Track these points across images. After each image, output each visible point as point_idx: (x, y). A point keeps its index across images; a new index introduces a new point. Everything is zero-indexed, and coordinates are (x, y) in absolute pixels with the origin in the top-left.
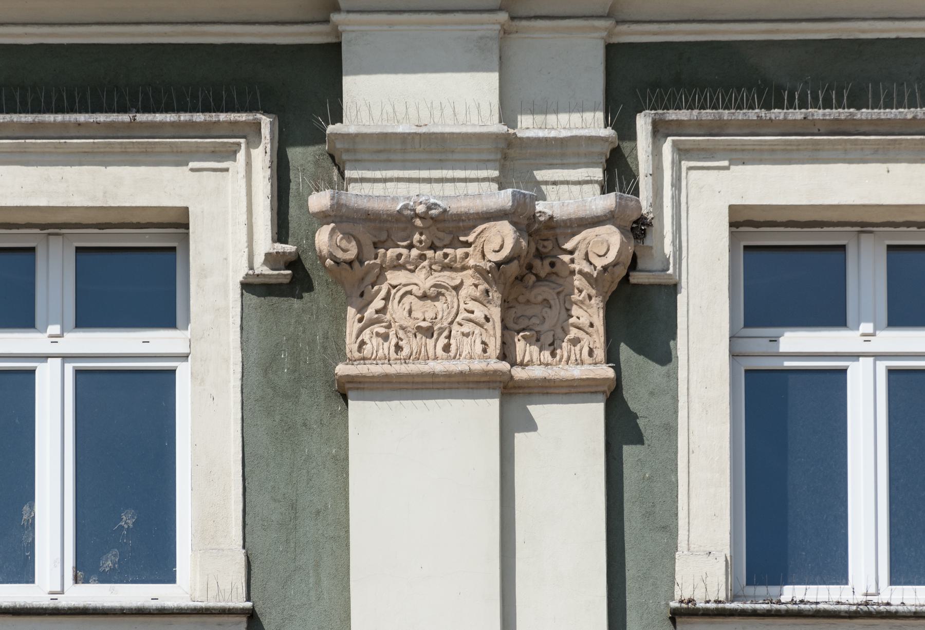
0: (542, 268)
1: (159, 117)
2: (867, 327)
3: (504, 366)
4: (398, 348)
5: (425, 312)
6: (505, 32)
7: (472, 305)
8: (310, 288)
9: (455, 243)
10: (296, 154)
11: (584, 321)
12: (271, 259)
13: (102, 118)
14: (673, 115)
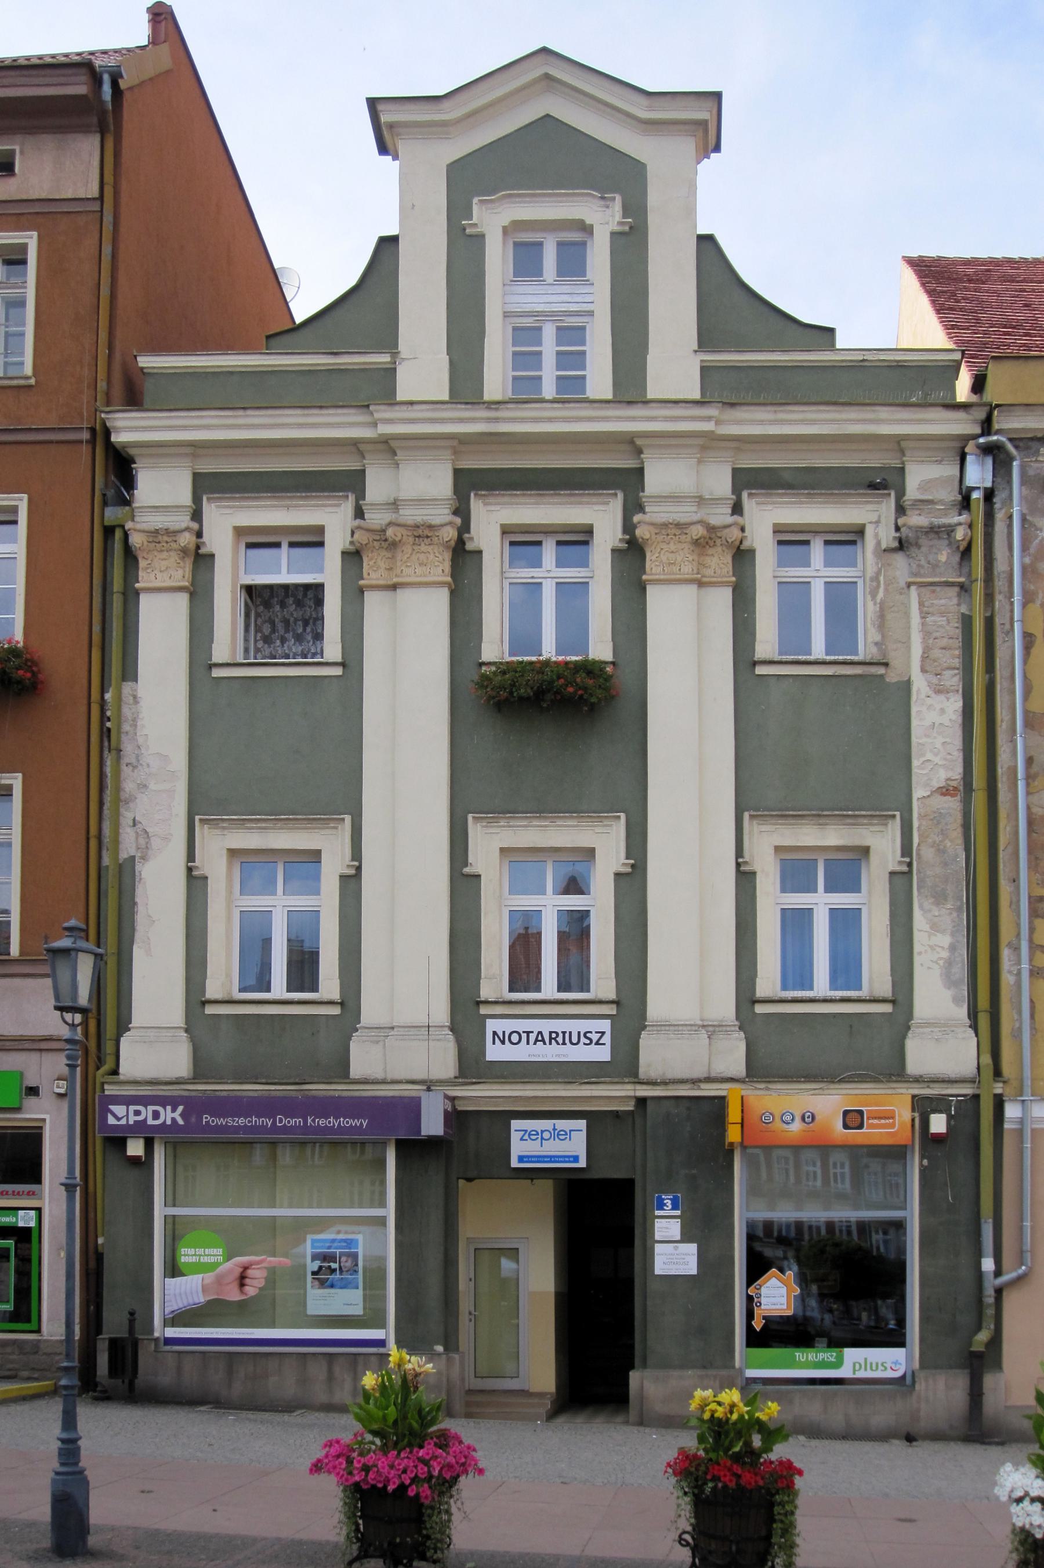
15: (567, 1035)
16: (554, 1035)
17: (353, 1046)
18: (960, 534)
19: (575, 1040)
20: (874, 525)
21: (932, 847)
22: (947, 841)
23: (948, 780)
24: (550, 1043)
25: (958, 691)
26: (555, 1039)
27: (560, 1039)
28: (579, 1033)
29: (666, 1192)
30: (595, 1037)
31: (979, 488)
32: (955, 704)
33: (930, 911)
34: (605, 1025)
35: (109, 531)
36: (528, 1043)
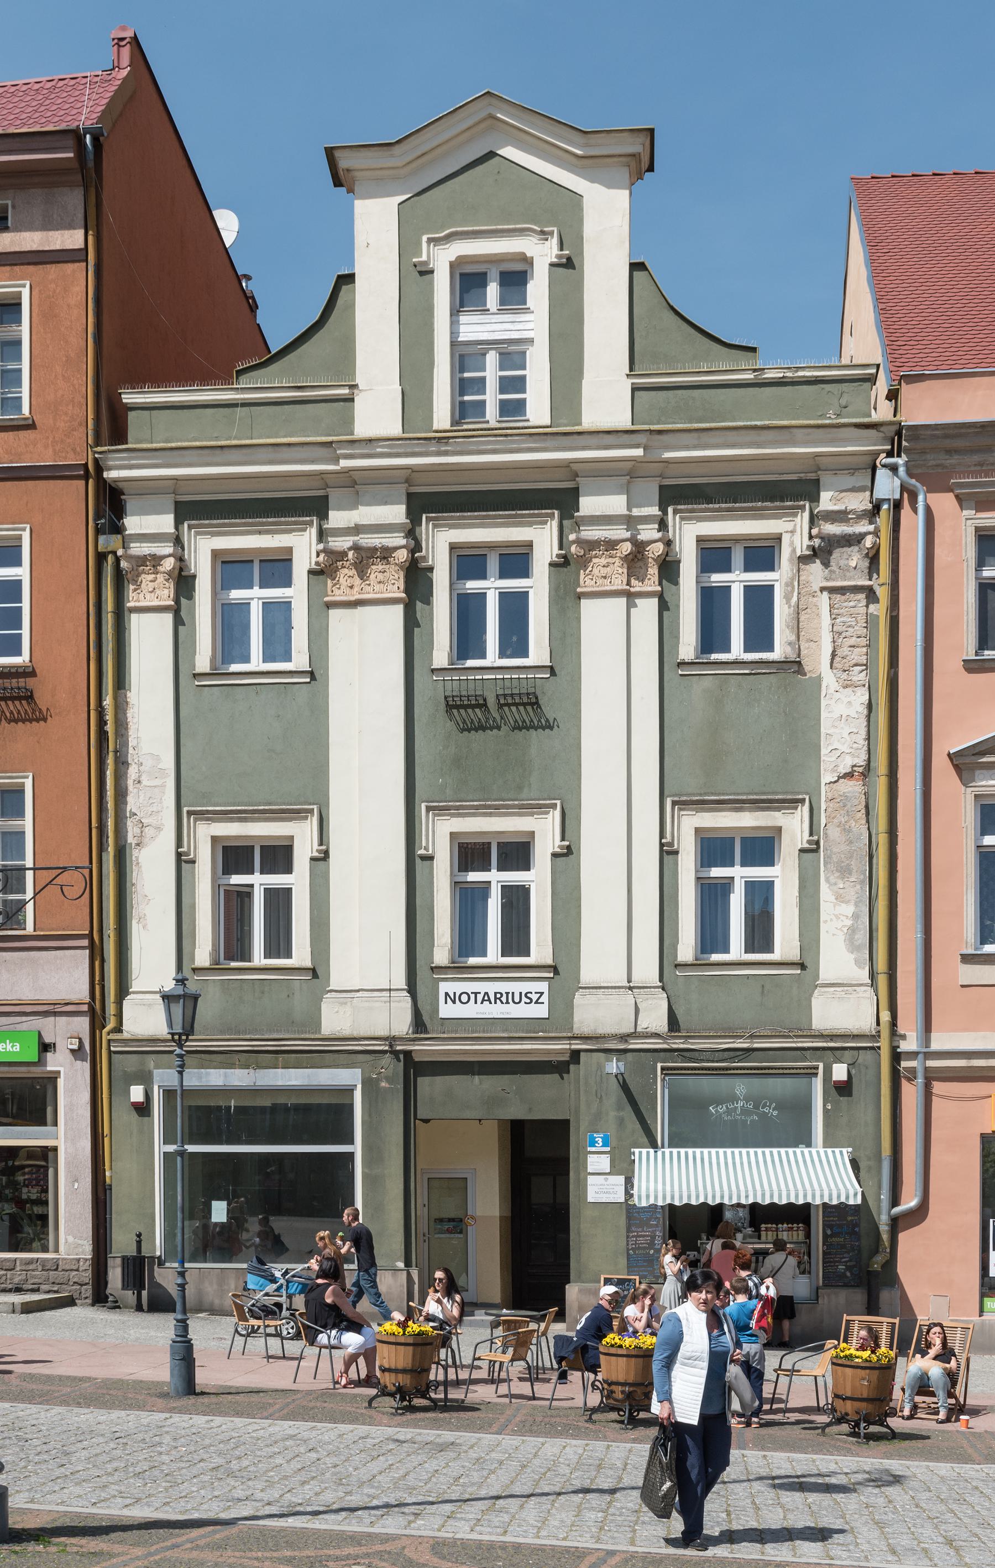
0: (640, 556)
1: (524, 512)
2: (737, 572)
3: (628, 587)
4: (596, 583)
5: (604, 571)
6: (629, 482)
7: (618, 569)
8: (570, 565)
9: (613, 549)
10: (565, 522)
11: (652, 573)
12: (558, 556)
13: (507, 513)
14: (679, 507)
15: (510, 996)
16: (498, 996)
17: (324, 1007)
18: (869, 541)
19: (517, 1000)
20: (790, 535)
21: (838, 826)
22: (852, 821)
23: (855, 766)
24: (495, 1003)
25: (864, 686)
26: (499, 999)
27: (504, 999)
28: (521, 993)
29: (597, 1132)
30: (534, 997)
31: (889, 500)
32: (862, 696)
33: (835, 884)
34: (543, 987)
35: (101, 557)
36: (476, 1002)
